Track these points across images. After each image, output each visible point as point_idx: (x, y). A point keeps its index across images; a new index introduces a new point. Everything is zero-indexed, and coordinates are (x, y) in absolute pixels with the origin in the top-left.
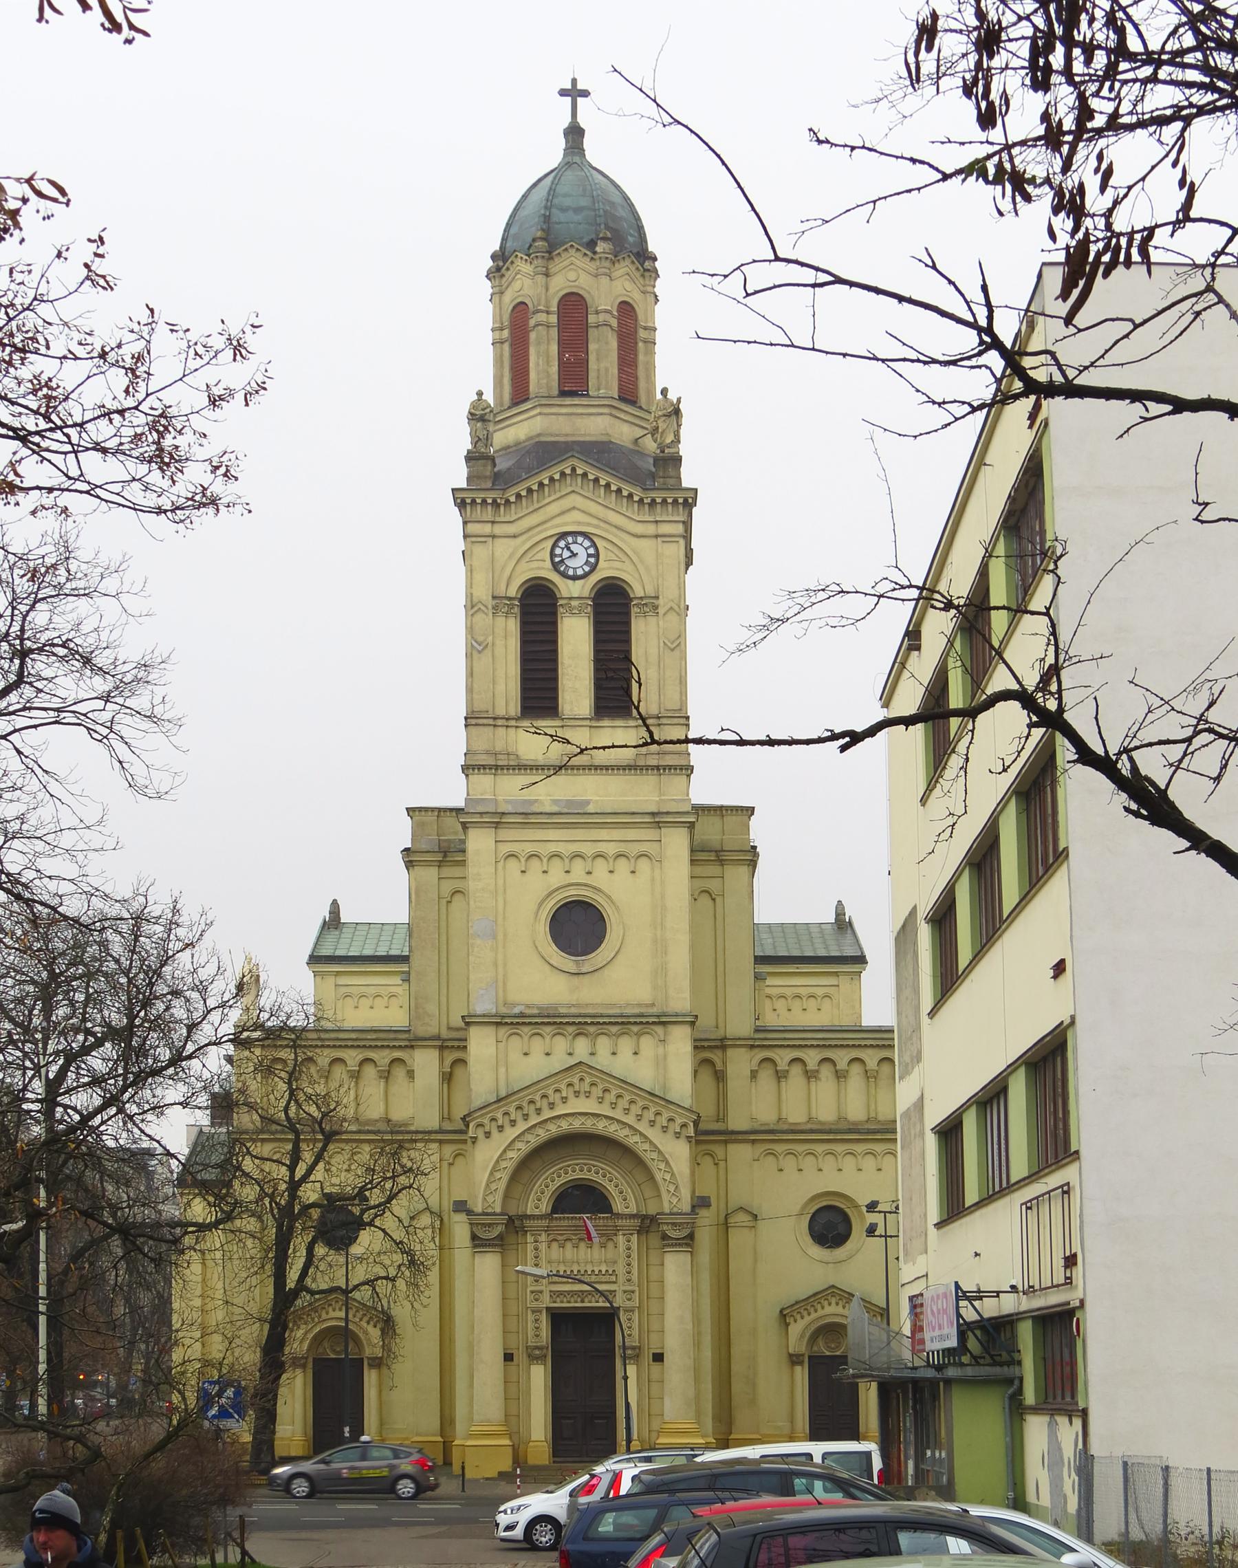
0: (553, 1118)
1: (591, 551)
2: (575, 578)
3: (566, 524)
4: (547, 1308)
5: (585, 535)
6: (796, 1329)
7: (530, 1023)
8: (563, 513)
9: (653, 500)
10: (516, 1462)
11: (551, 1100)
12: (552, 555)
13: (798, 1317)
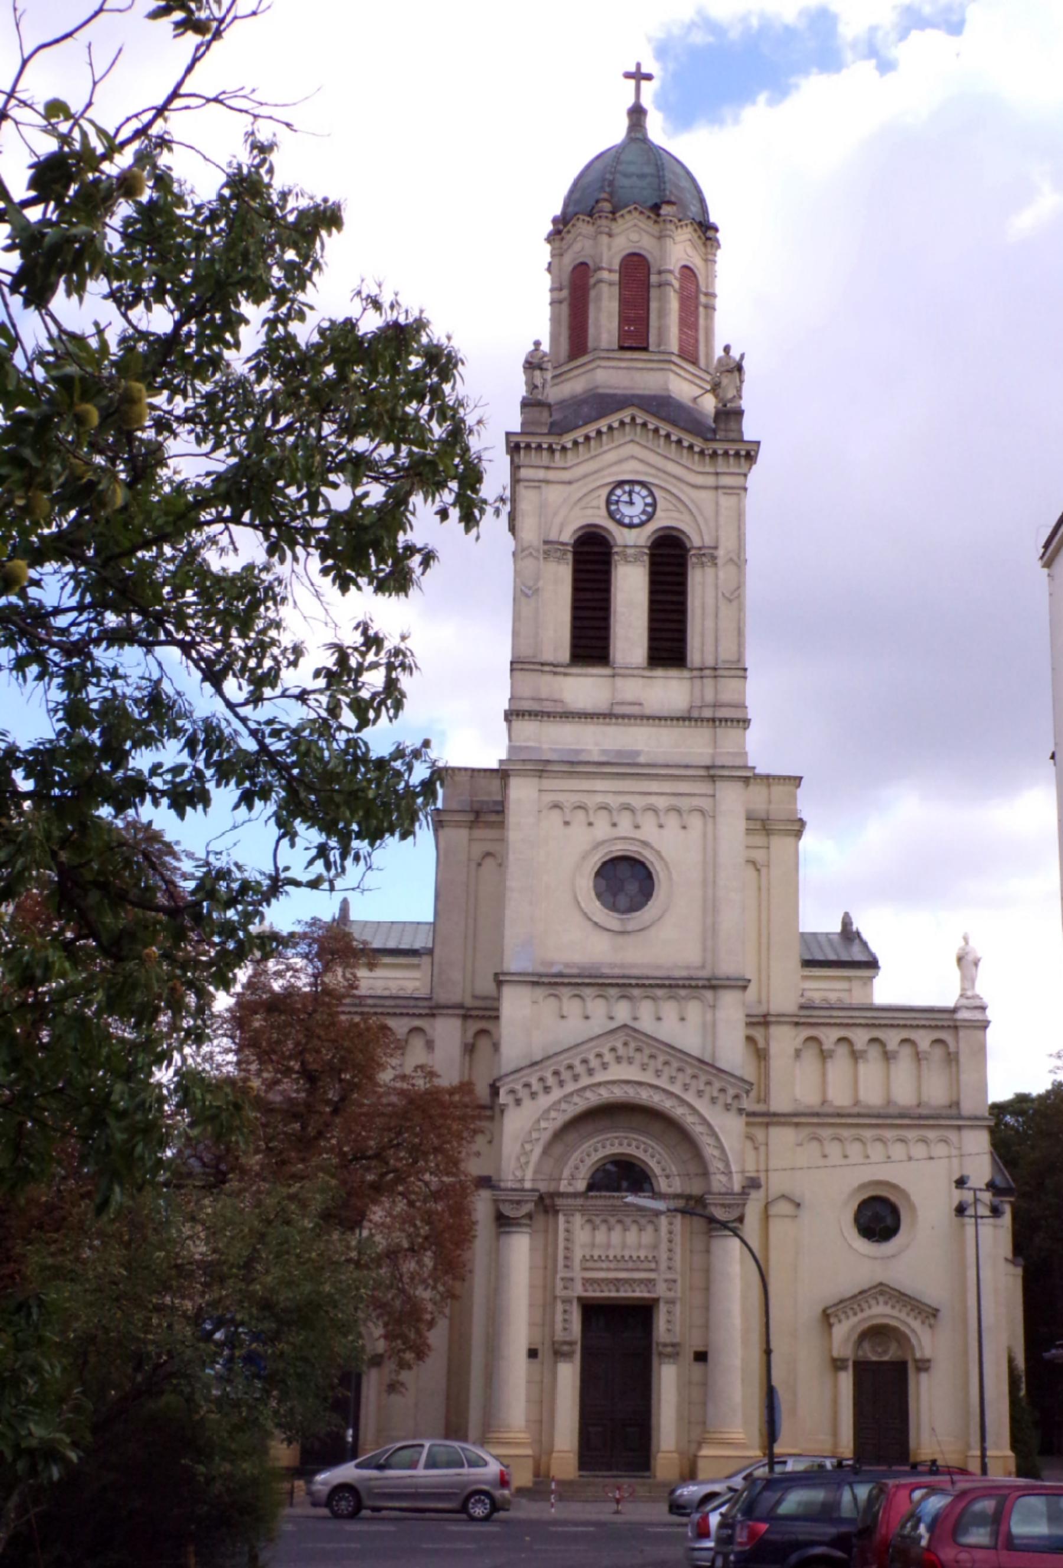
1: (649, 500)
2: (631, 526)
3: (623, 472)
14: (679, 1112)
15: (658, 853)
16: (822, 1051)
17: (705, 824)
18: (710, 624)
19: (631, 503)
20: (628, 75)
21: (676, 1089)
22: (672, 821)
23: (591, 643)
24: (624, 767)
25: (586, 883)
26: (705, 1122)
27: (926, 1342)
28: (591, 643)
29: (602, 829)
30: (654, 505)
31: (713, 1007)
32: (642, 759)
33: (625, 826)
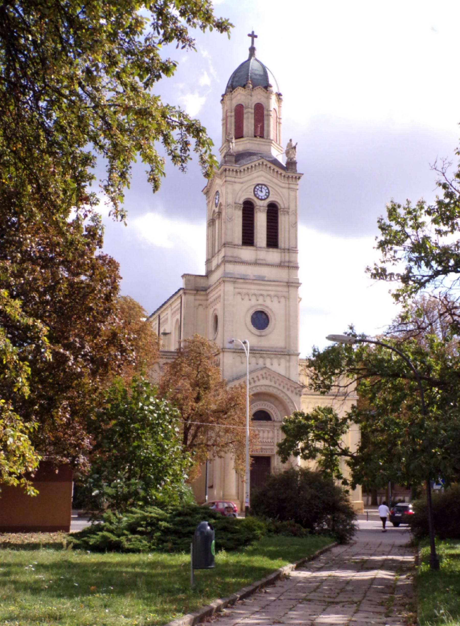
2: (262, 200)
5: (265, 185)
14: (281, 395)
15: (271, 310)
18: (287, 234)
19: (261, 191)
20: (249, 35)
21: (281, 388)
22: (275, 300)
23: (248, 239)
25: (249, 319)
26: (289, 398)
29: (254, 302)
30: (269, 193)
31: (289, 361)
32: (266, 279)
33: (261, 301)
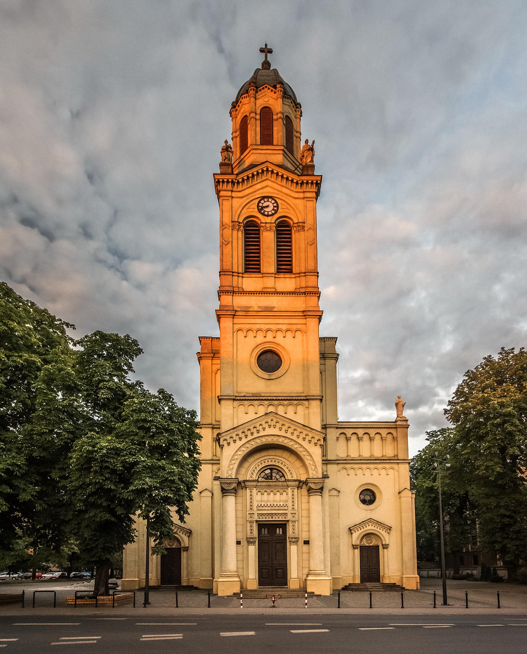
0: (259, 437)
1: (275, 205)
2: (268, 216)
3: (264, 193)
4: (256, 521)
5: (271, 197)
6: (356, 535)
7: (248, 400)
8: (263, 188)
9: (303, 182)
10: (242, 587)
11: (258, 429)
12: (258, 206)
13: (356, 530)
15: (283, 348)
16: (346, 438)
17: (303, 336)
18: (303, 255)
24: (268, 312)
27: (386, 538)
28: (252, 264)
29: (260, 339)
30: (277, 207)
32: (275, 310)
33: (270, 337)
